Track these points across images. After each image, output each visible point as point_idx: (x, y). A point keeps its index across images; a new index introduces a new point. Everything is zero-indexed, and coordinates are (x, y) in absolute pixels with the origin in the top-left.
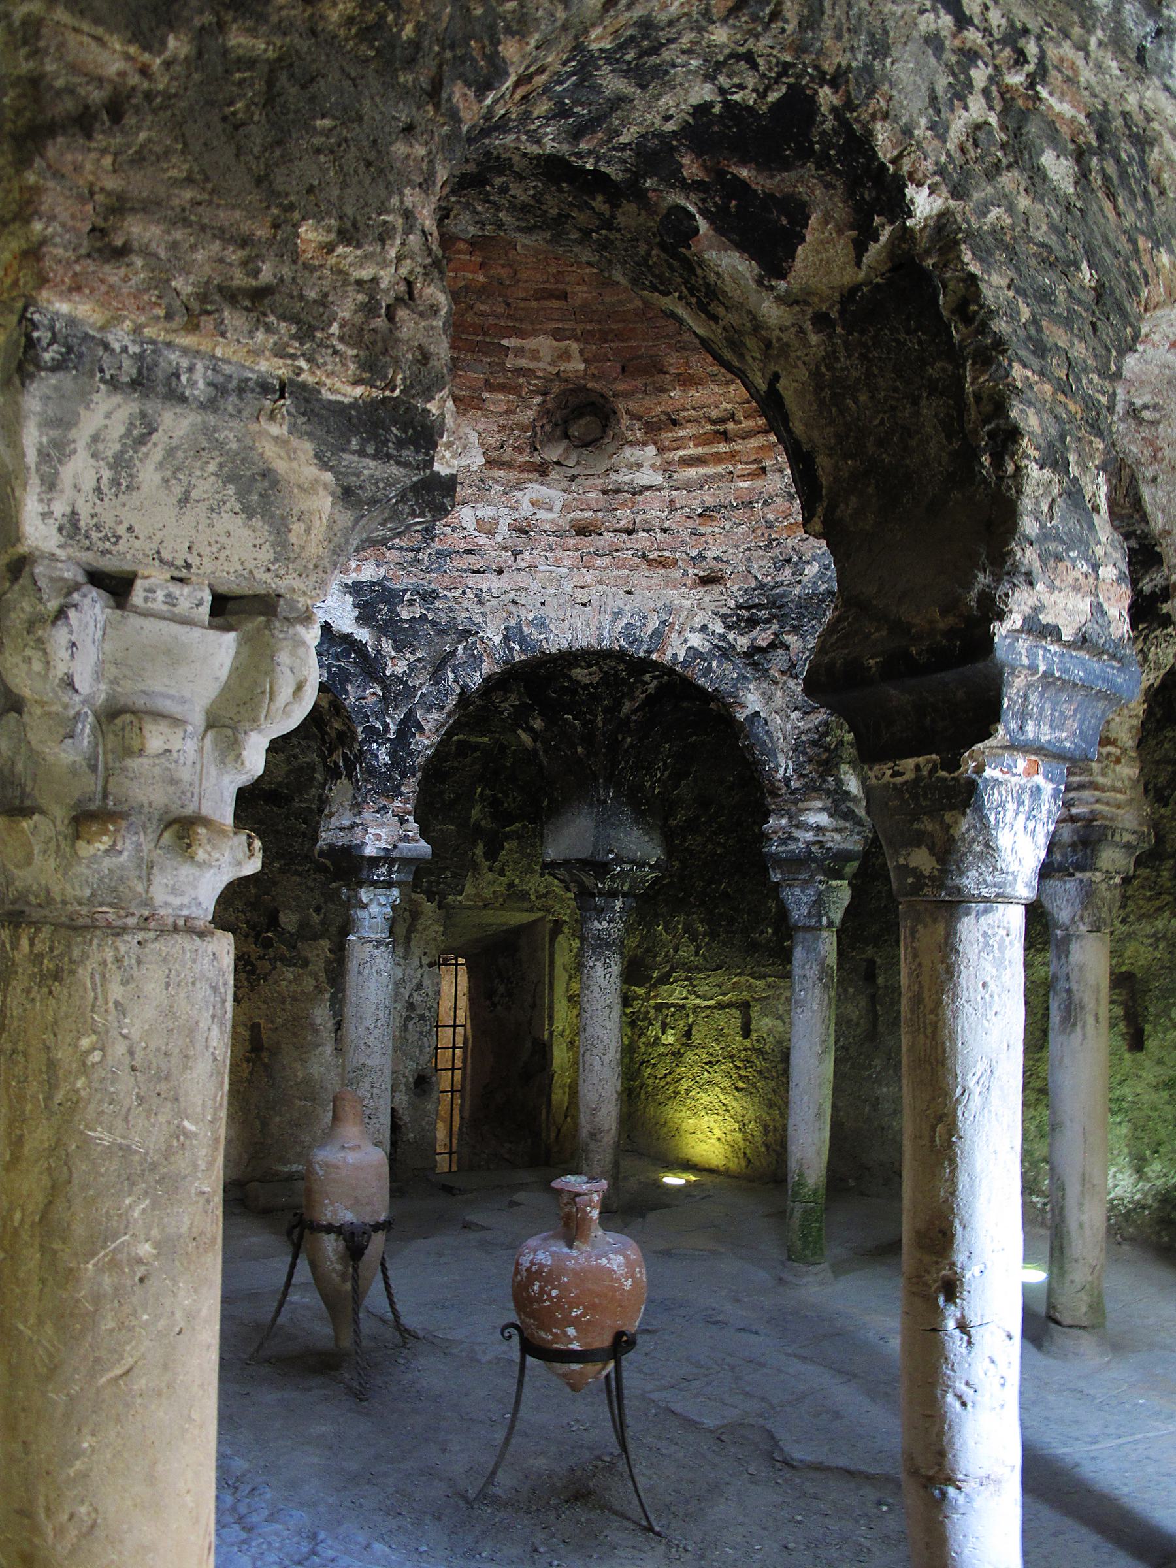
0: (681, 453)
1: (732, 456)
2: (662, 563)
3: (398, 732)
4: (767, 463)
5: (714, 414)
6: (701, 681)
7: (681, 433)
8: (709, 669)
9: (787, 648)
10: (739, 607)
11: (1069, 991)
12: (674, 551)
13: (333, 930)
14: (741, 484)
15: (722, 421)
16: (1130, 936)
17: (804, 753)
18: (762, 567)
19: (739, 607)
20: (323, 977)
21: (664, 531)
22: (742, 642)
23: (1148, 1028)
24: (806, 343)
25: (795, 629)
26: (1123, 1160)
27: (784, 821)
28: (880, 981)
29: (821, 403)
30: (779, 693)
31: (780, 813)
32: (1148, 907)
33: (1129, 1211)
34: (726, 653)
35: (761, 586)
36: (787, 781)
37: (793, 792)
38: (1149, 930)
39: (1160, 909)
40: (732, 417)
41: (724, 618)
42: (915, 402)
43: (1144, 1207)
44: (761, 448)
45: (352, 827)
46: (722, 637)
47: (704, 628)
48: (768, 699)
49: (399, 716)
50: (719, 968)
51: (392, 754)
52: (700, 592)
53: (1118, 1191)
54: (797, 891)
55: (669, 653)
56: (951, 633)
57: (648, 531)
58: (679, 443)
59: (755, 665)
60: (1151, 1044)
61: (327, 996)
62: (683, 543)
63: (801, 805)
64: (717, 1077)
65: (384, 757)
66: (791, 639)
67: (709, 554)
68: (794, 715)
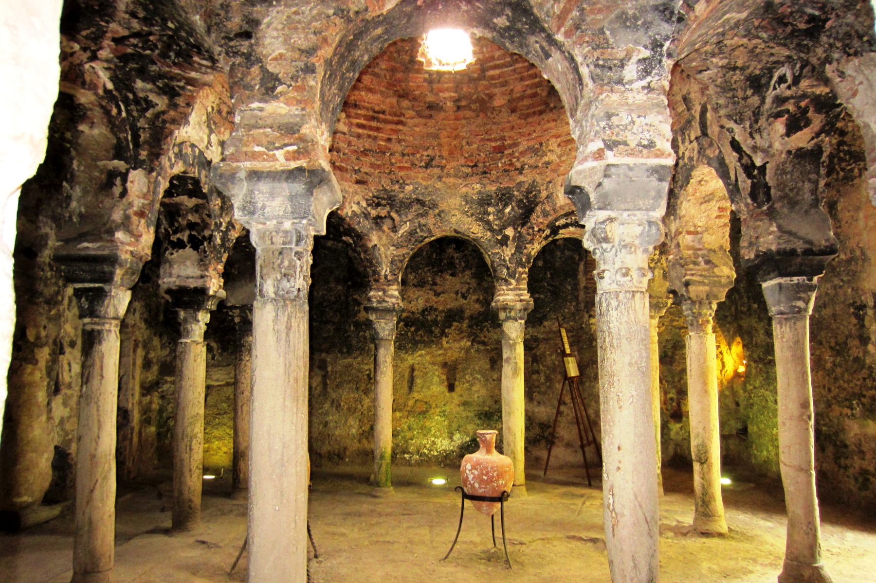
0: (358, 121)
1: (378, 129)
2: (340, 169)
3: (227, 228)
4: (394, 137)
5: (377, 108)
6: (356, 227)
7: (359, 112)
8: (359, 222)
9: (393, 220)
10: (374, 197)
11: (516, 363)
12: (347, 165)
13: (51, 341)
14: (381, 143)
15: (378, 112)
16: (450, 348)
17: (396, 265)
18: (386, 183)
19: (374, 197)
20: (44, 372)
21: (344, 154)
22: (374, 213)
23: (457, 383)
24: (780, 156)
25: (397, 212)
26: (445, 435)
27: (380, 293)
28: (329, 369)
29: (776, 174)
30: (384, 238)
31: (378, 290)
32: (458, 338)
33: (447, 455)
34: (366, 216)
35: (385, 190)
36: (386, 276)
37: (389, 281)
38: (458, 346)
39: (463, 338)
40: (383, 112)
41: (367, 200)
42: (803, 182)
43: (453, 452)
44: (392, 130)
45: (202, 277)
46: (366, 209)
47: (358, 203)
48: (380, 238)
49: (227, 219)
50: (228, 365)
51: (223, 239)
52: (356, 186)
53: (443, 447)
54: (383, 325)
55: (345, 211)
56: (826, 247)
57: (338, 152)
58: (358, 116)
59: (377, 224)
60: (458, 389)
61: (46, 383)
62: (352, 162)
63: (391, 287)
64: (226, 420)
65: (218, 241)
66: (394, 215)
67: (362, 170)
68: (392, 248)
